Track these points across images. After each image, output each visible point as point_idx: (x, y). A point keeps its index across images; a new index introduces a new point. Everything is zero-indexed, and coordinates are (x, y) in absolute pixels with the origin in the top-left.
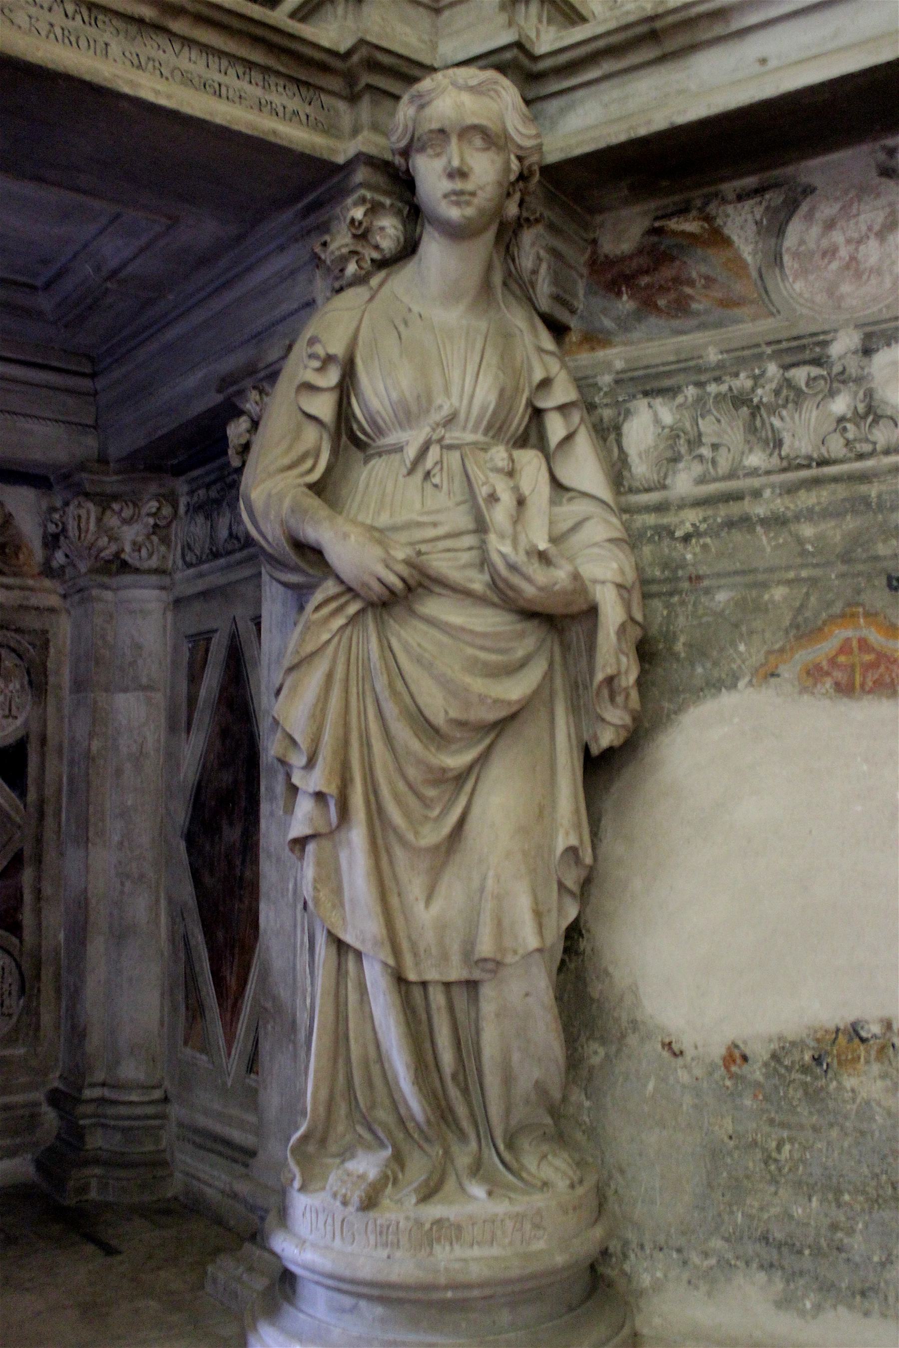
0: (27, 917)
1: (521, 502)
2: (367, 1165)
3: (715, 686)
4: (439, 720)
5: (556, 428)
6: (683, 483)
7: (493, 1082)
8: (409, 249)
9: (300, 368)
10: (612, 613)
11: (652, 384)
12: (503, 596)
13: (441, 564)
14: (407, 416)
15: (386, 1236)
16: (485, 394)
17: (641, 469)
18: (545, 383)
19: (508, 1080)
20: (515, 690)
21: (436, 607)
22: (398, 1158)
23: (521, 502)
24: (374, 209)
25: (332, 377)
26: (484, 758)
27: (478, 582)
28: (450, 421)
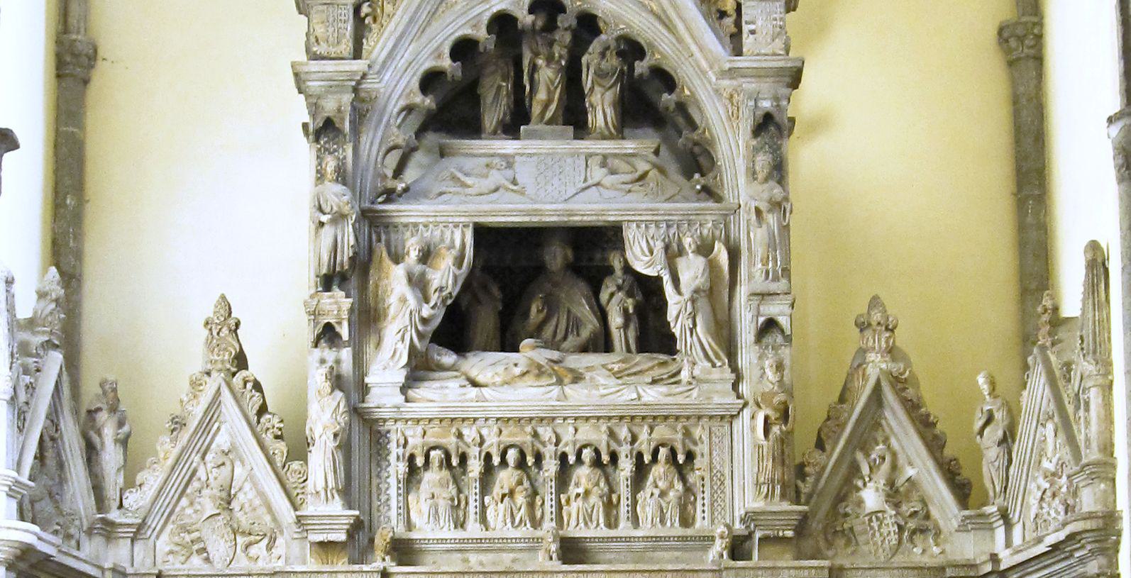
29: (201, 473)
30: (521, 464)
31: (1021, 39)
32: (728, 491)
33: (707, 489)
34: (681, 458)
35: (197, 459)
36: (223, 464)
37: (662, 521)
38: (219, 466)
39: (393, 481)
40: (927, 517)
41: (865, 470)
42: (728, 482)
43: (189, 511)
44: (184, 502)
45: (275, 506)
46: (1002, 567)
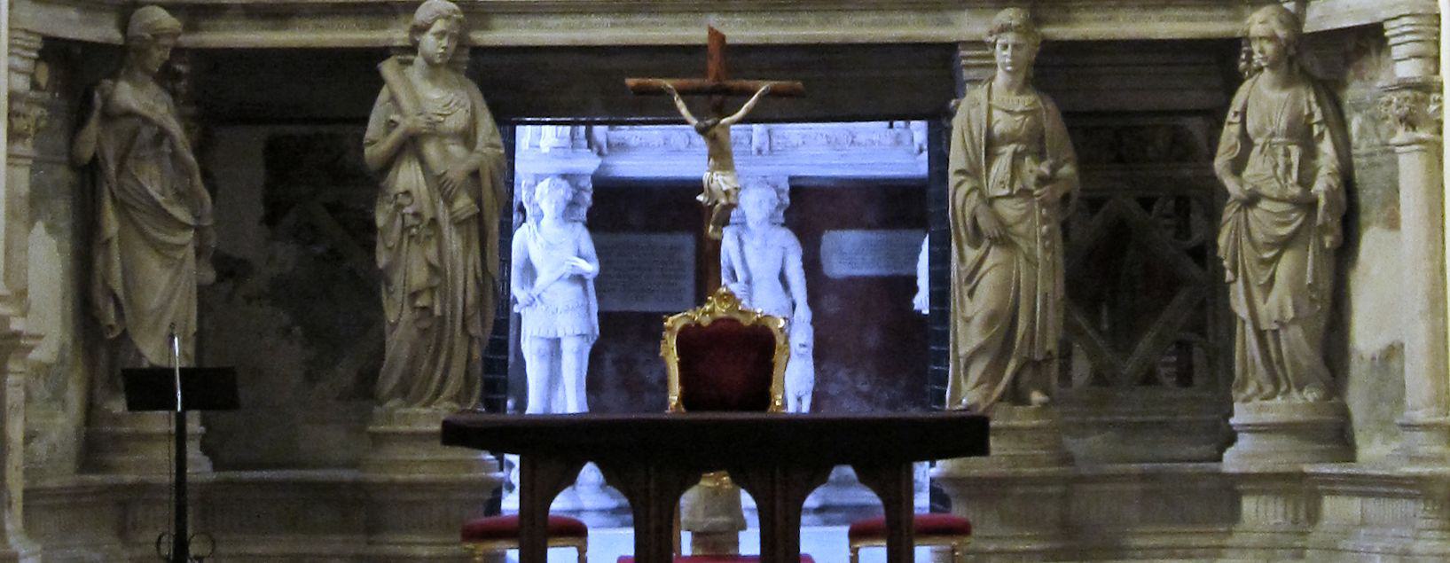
0: (1210, 330)
3: (1369, 224)
5: (1316, 131)
6: (1363, 149)
7: (1288, 366)
9: (1230, 117)
10: (1322, 202)
11: (1357, 108)
13: (1264, 190)
14: (1259, 134)
16: (1283, 125)
17: (1355, 140)
19: (1295, 364)
20: (1284, 231)
21: (1264, 205)
23: (1288, 167)
25: (1238, 119)
26: (1276, 258)
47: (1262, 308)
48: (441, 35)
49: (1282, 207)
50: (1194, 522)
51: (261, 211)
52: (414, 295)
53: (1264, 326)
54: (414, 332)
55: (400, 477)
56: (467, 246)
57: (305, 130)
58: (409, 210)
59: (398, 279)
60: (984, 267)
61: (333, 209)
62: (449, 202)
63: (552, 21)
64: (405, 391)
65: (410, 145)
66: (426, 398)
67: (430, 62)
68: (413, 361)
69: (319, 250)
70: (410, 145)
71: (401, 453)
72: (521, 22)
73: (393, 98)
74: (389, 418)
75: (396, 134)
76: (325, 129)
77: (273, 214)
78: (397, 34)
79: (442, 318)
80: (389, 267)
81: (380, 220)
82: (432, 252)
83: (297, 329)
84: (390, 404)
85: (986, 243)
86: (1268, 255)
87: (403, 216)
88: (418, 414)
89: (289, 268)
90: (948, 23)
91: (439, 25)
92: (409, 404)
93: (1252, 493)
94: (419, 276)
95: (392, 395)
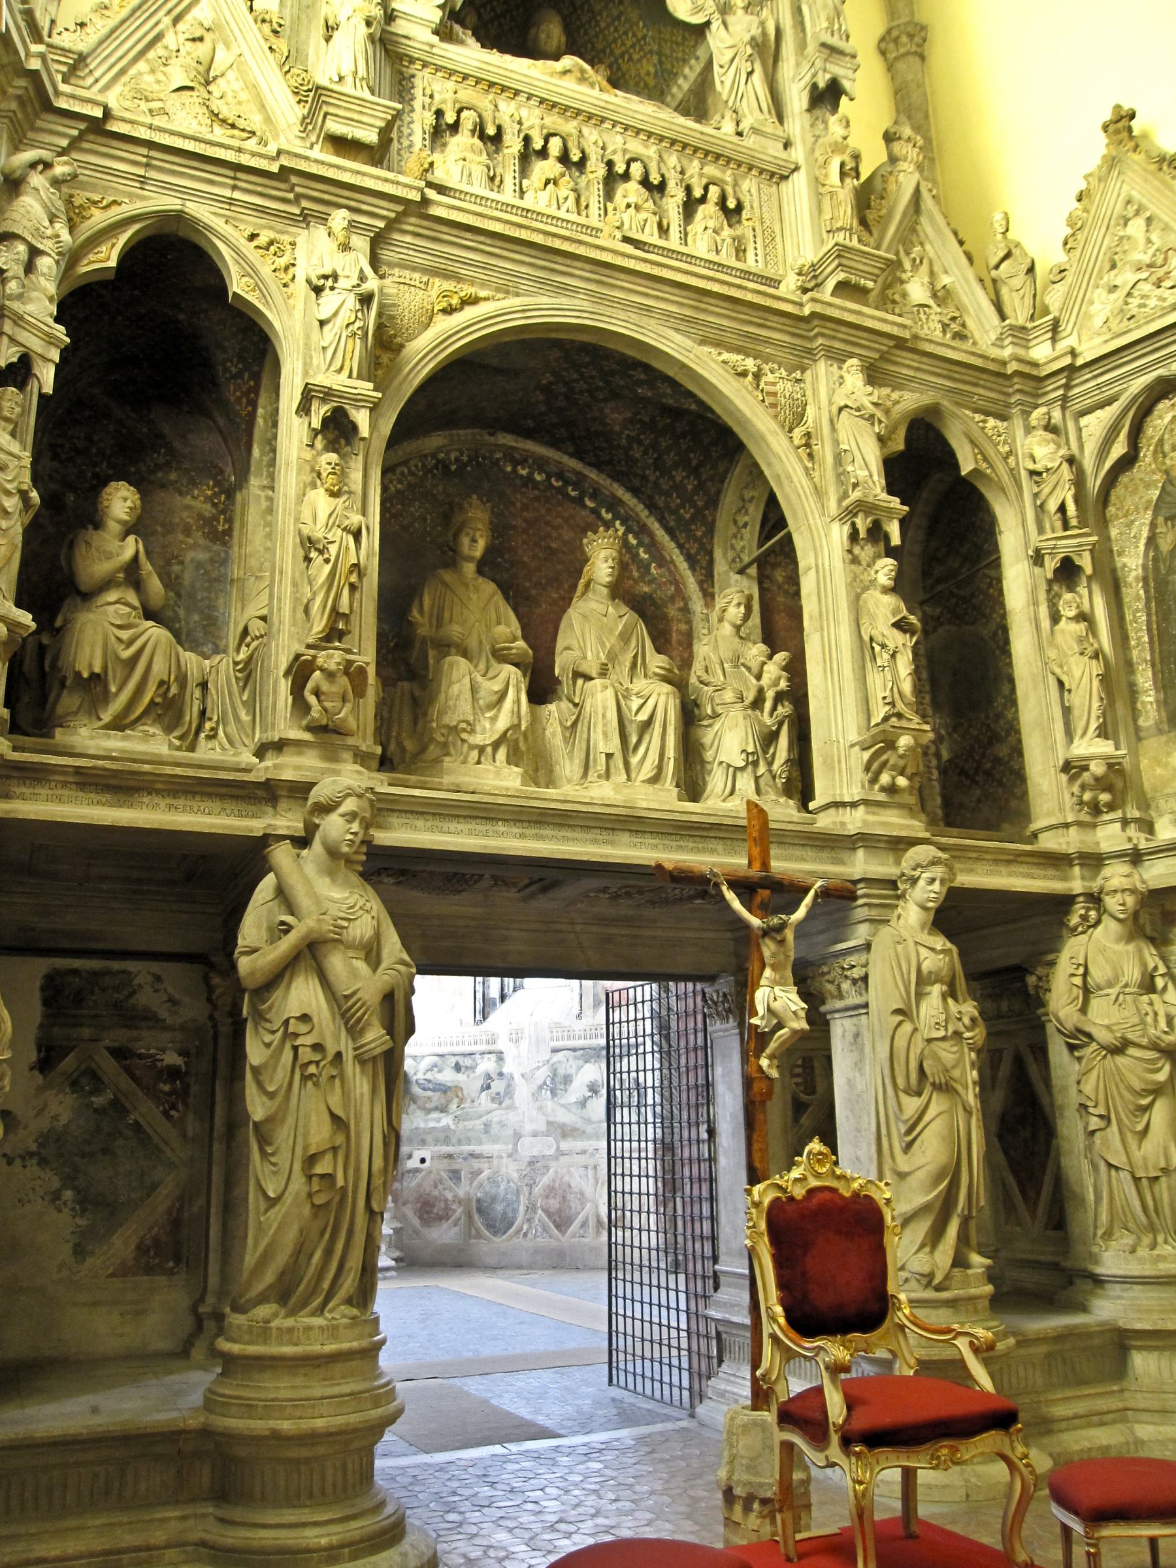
1: (1156, 1014)
2: (1129, 1240)
4: (1138, 1089)
8: (1098, 922)
12: (1154, 1046)
13: (1130, 1036)
15: (1141, 1261)
18: (1156, 968)
21: (1131, 1051)
22: (1139, 1238)
23: (1156, 1014)
24: (1088, 909)
25: (1081, 970)
26: (1153, 1102)
27: (1144, 1042)
28: (1126, 986)
29: (170, 40)
30: (564, 158)
31: (911, 36)
32: (780, 246)
33: (759, 240)
34: (732, 204)
35: (167, 20)
36: (201, 39)
37: (718, 252)
38: (194, 40)
39: (417, 128)
40: (964, 325)
41: (907, 265)
42: (778, 239)
43: (149, 78)
44: (142, 66)
45: (269, 100)
46: (1080, 362)
47: (1137, 1155)
48: (352, 816)
49: (1152, 1055)
50: (1081, 1382)
51: (33, 1056)
52: (311, 1160)
53: (1140, 1174)
54: (307, 1211)
55: (286, 1426)
56: (374, 1091)
57: (95, 964)
58: (309, 1040)
59: (283, 1135)
60: (927, 1118)
61: (120, 1053)
62: (354, 1030)
63: (453, 826)
64: (284, 1293)
65: (310, 954)
66: (317, 1302)
67: (333, 852)
68: (301, 1252)
69: (98, 1101)
70: (310, 954)
71: (282, 1387)
72: (420, 823)
73: (282, 893)
74: (263, 1332)
75: (291, 939)
76: (116, 965)
77: (48, 1058)
78: (287, 821)
79: (344, 1189)
80: (269, 1120)
81: (255, 1053)
82: (335, 1101)
83: (68, 1194)
84: (263, 1311)
85: (928, 1089)
86: (1145, 1102)
87: (295, 1049)
88: (309, 1328)
89: (63, 1120)
90: (842, 862)
91: (350, 805)
92: (292, 1313)
93: (1140, 1348)
94: (320, 1133)
95: (262, 1299)
